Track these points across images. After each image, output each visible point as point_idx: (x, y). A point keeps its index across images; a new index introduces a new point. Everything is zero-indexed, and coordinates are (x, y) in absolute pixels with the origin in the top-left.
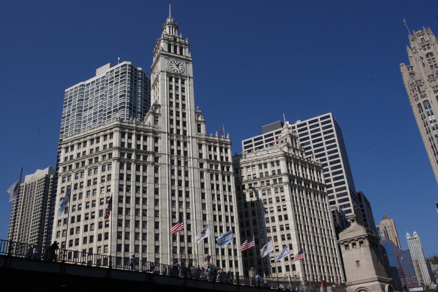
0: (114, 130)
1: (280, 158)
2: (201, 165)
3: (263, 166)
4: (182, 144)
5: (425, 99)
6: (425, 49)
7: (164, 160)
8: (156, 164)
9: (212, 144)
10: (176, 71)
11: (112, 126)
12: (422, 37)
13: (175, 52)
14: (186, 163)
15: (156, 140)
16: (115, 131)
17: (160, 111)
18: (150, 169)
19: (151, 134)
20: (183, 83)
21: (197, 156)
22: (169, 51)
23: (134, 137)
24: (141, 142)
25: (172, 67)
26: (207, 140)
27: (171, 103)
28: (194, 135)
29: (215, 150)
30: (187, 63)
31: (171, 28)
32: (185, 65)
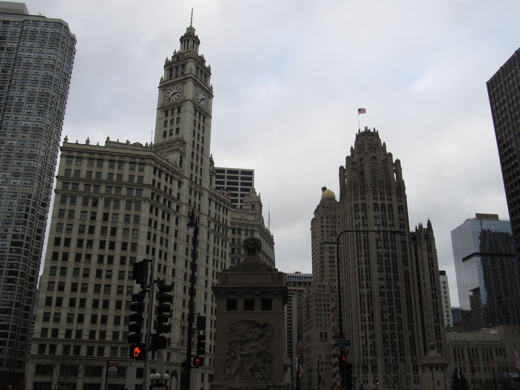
0: (147, 161)
1: (255, 229)
3: (236, 232)
5: (363, 201)
6: (371, 151)
8: (177, 214)
11: (146, 156)
12: (370, 137)
15: (180, 183)
16: (150, 164)
17: (185, 150)
18: (173, 219)
19: (177, 177)
20: (204, 121)
23: (163, 176)
28: (207, 188)
30: (209, 98)
31: (195, 43)
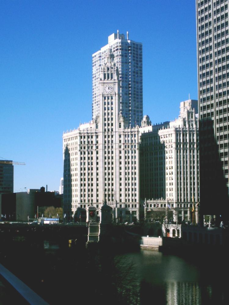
2: (120, 147)
4: (110, 137)
7: (101, 147)
8: (97, 150)
9: (127, 133)
10: (108, 92)
13: (108, 78)
14: (112, 147)
15: (97, 137)
17: (99, 120)
18: (95, 153)
20: (112, 99)
21: (118, 142)
22: (105, 78)
24: (90, 140)
25: (105, 90)
26: (123, 132)
27: (105, 114)
29: (128, 137)
32: (113, 86)
